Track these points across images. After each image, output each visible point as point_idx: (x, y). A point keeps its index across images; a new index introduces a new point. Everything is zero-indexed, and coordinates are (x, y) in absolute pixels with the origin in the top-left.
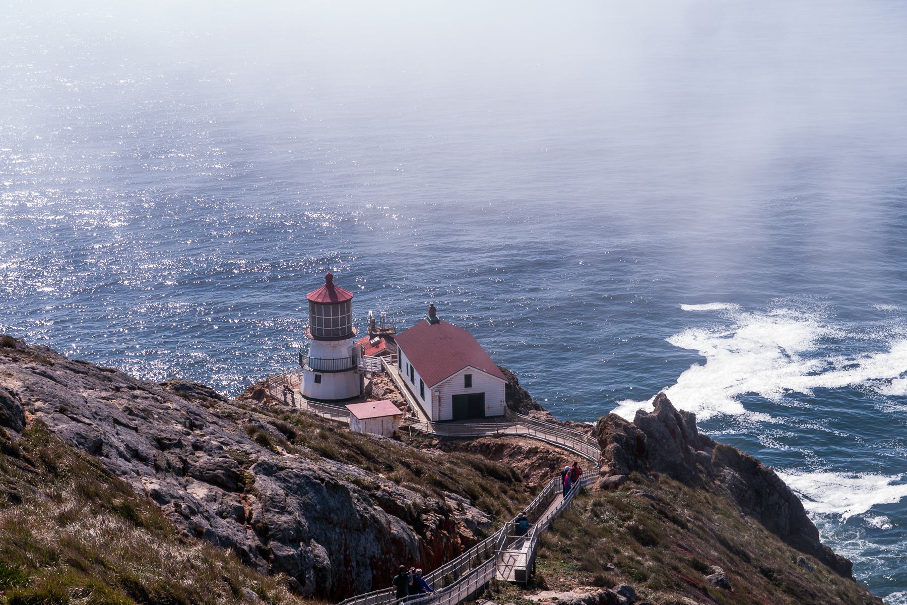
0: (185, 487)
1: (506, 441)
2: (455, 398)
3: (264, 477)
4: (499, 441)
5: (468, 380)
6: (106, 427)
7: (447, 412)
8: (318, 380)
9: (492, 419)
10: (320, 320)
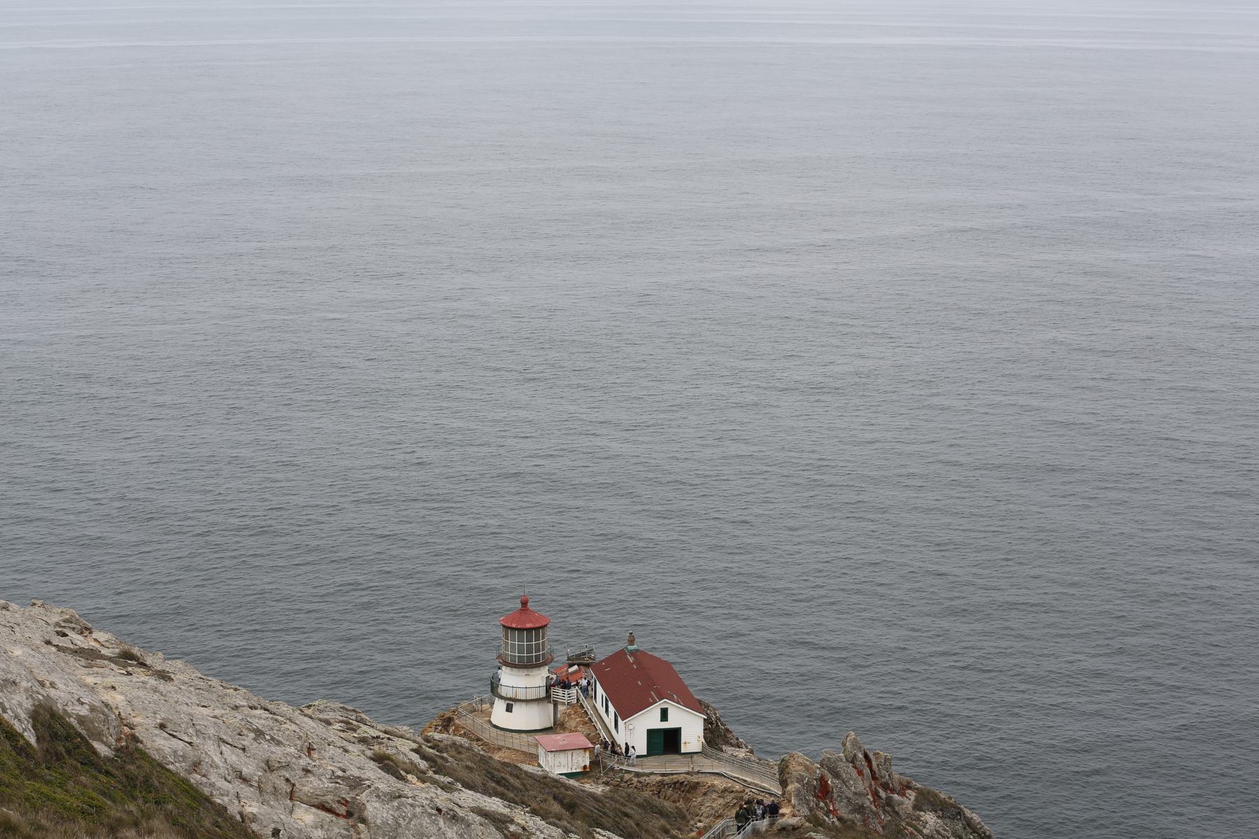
0: (291, 812)
1: (701, 779)
3: (377, 805)
4: (695, 779)
6: (211, 748)
8: (509, 709)
10: (513, 645)
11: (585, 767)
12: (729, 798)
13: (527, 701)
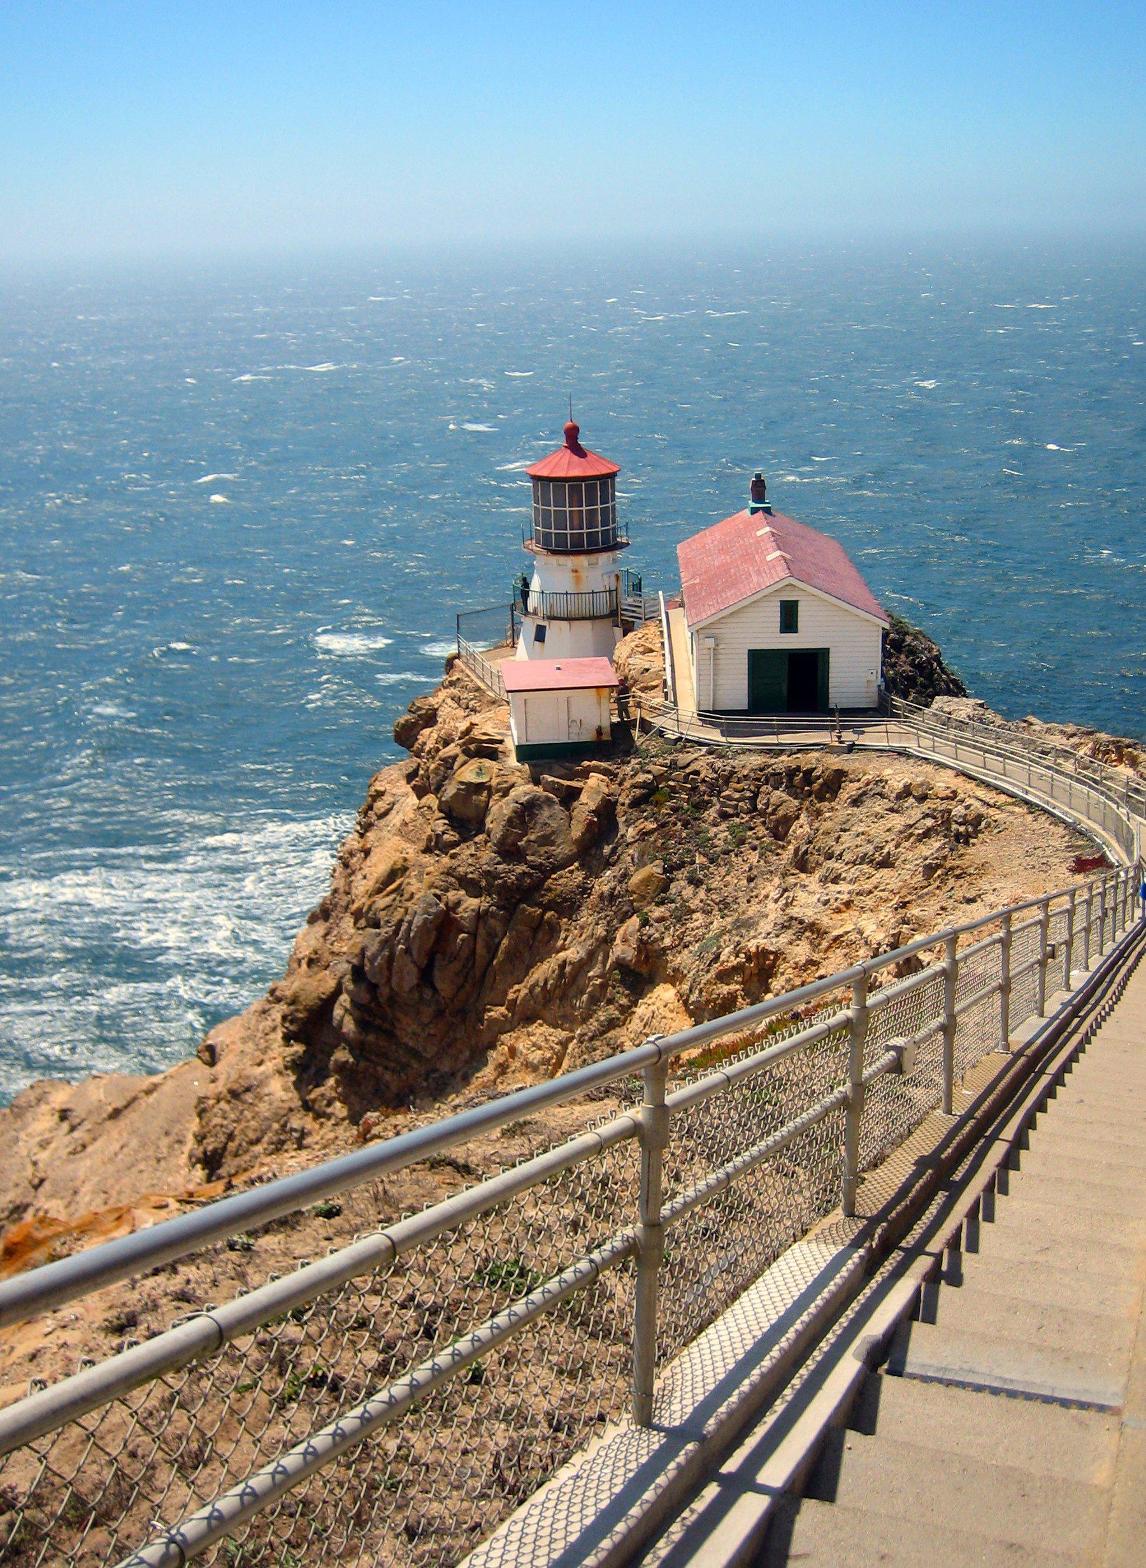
2: (756, 657)
4: (835, 762)
5: (789, 618)
7: (736, 690)
9: (831, 712)
10: (546, 513)
11: (599, 731)
12: (914, 812)
13: (569, 619)
